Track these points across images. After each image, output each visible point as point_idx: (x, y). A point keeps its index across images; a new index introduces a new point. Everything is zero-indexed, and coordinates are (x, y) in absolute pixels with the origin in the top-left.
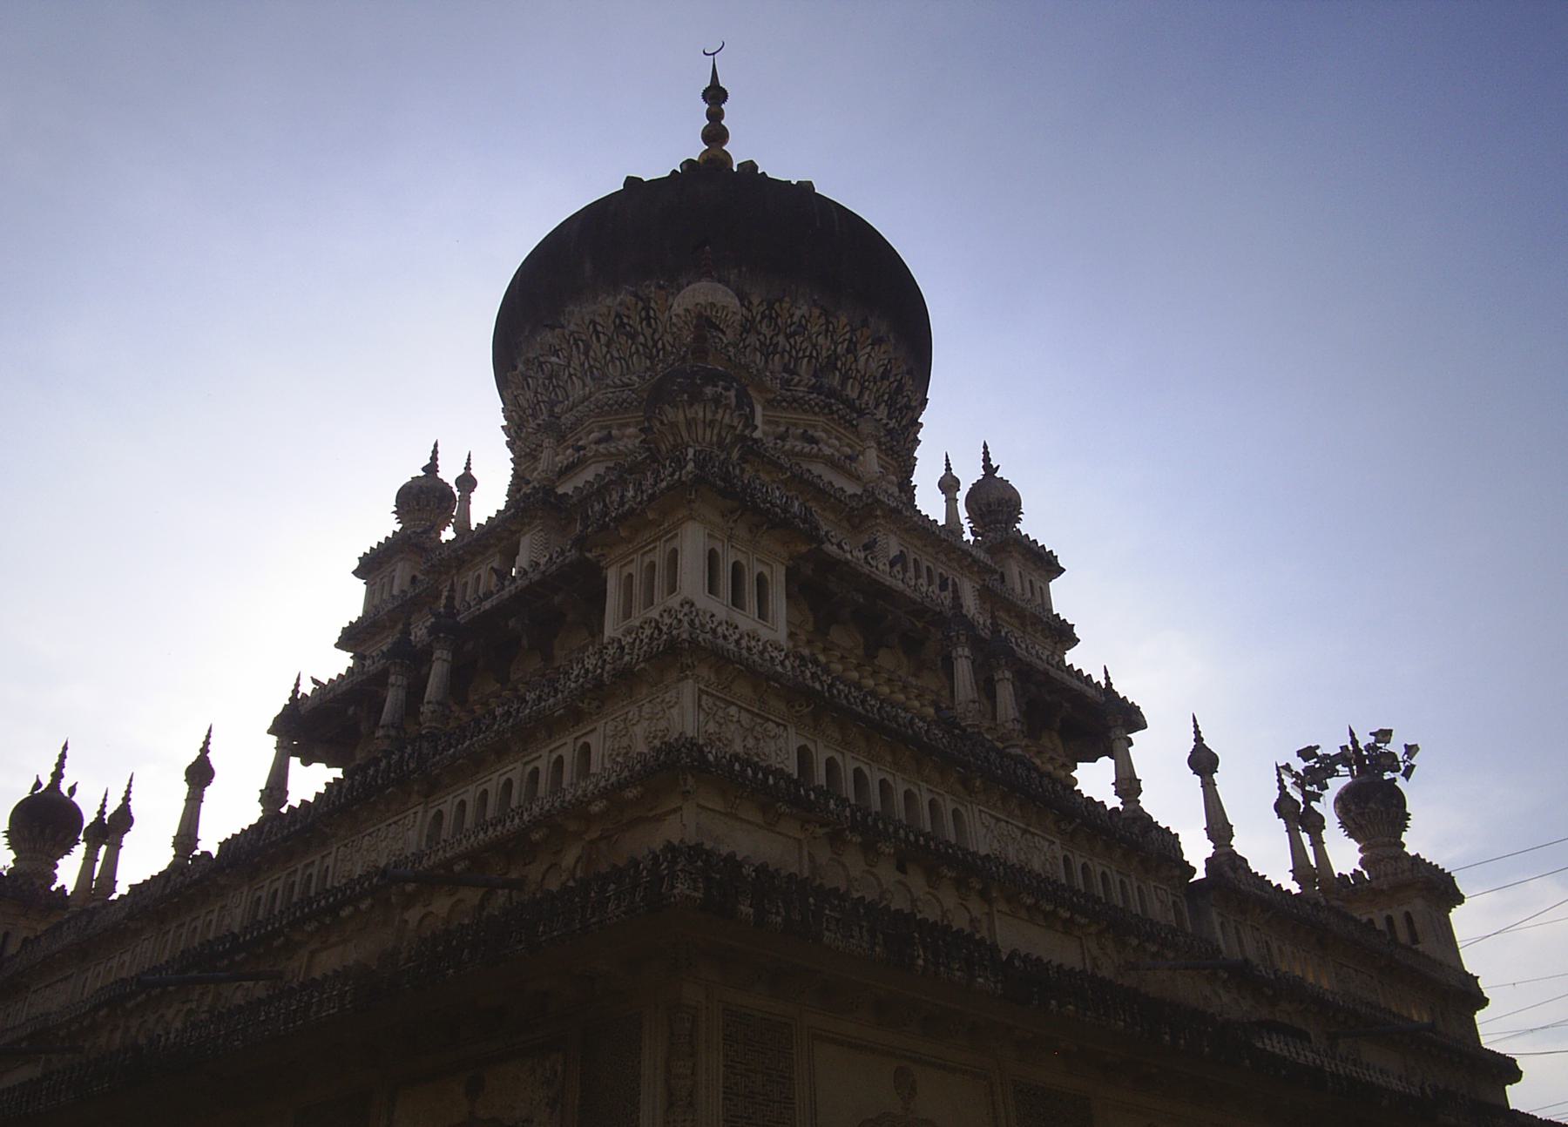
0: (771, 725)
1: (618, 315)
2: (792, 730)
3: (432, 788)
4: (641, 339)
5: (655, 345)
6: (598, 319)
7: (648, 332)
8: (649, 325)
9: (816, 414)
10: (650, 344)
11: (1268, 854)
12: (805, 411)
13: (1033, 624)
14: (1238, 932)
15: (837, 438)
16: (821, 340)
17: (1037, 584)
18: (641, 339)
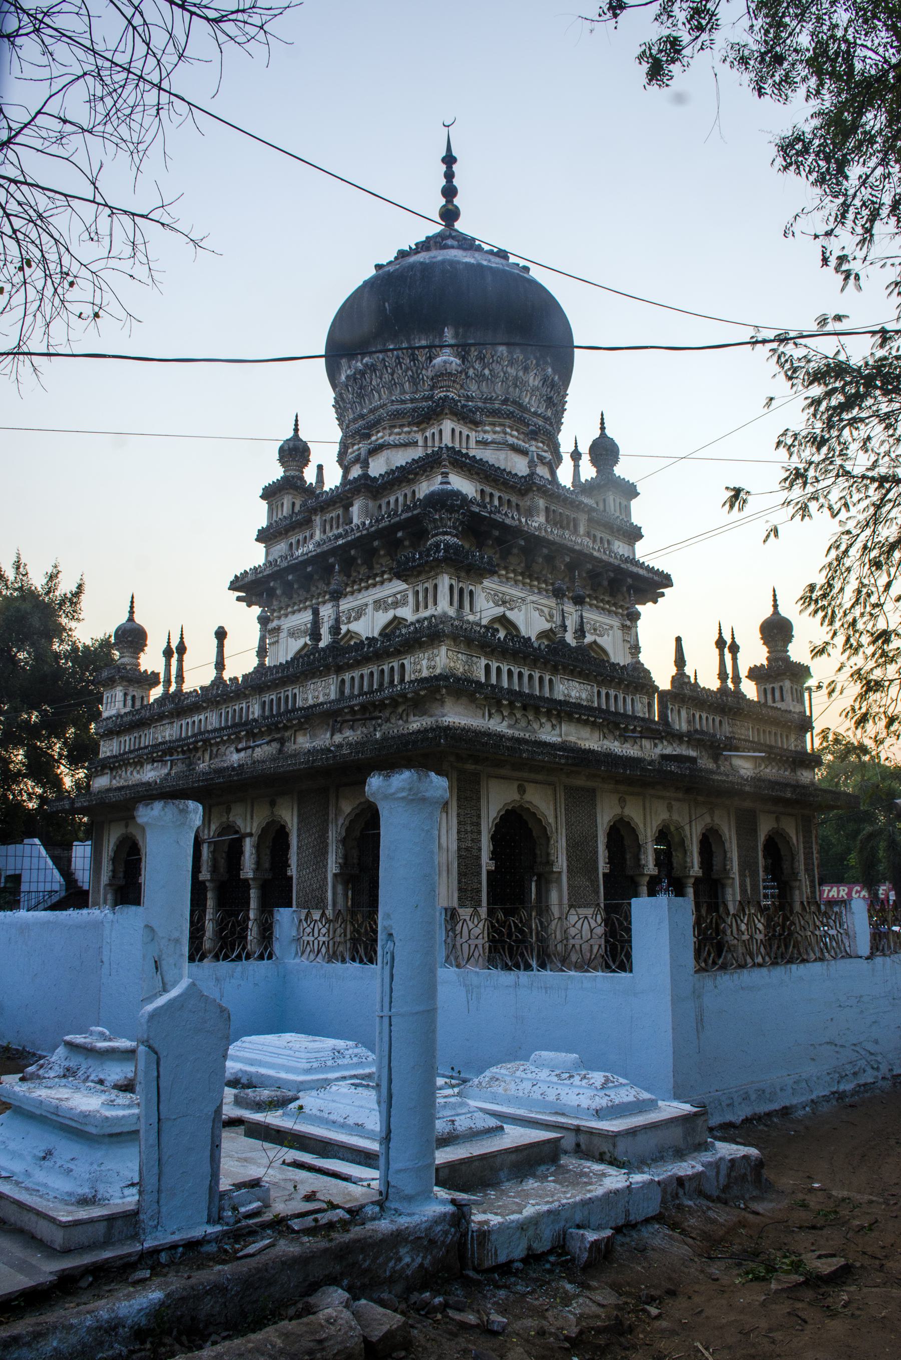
4: (410, 373)
7: (414, 369)
16: (509, 369)
18: (410, 373)
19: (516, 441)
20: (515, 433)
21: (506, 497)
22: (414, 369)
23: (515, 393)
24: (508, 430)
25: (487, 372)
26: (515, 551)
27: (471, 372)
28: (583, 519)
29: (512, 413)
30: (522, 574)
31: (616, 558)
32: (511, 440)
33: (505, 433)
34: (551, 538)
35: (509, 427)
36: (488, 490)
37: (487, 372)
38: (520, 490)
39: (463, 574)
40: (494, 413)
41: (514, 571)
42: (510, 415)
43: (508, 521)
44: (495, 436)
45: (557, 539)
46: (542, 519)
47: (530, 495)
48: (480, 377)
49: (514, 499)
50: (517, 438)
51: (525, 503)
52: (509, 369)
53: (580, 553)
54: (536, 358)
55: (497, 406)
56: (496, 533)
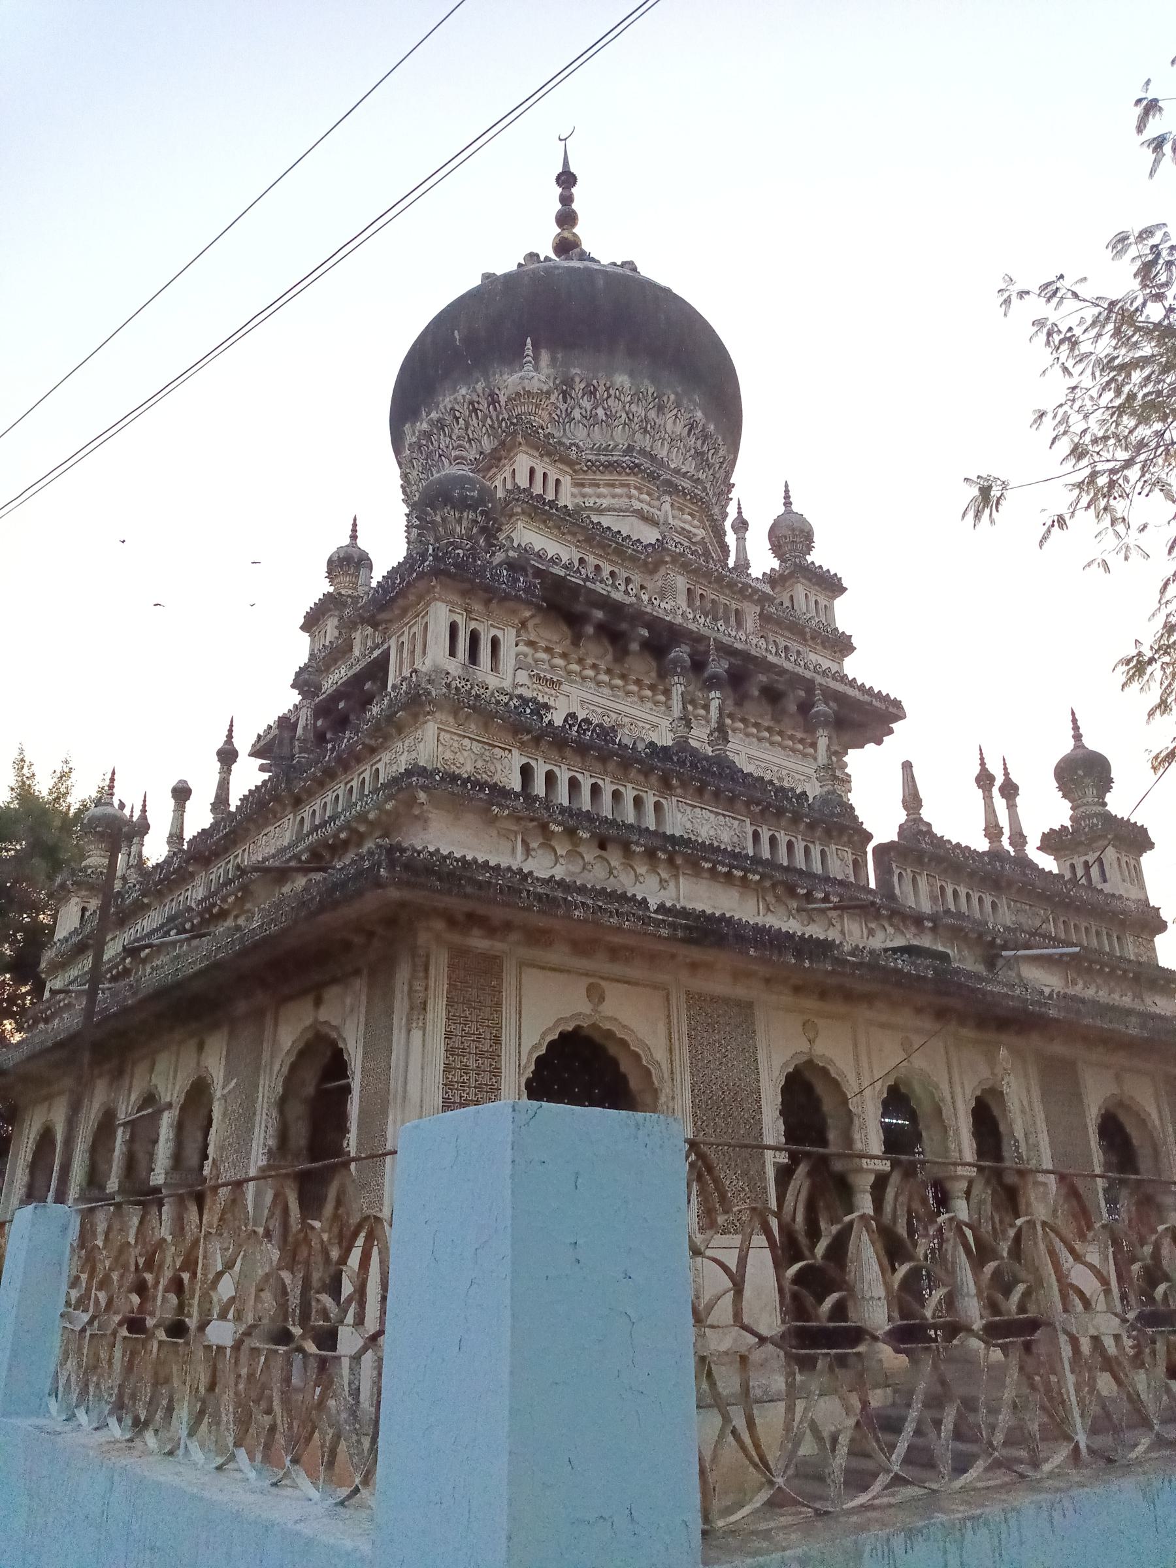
0: (497, 750)
1: (471, 403)
2: (515, 752)
3: (298, 802)
4: (489, 421)
5: (500, 427)
6: (457, 407)
7: (494, 414)
8: (495, 409)
9: (628, 475)
10: (496, 425)
11: (959, 822)
12: (619, 473)
13: (813, 638)
14: (914, 880)
15: (648, 494)
16: (634, 408)
17: (823, 602)
18: (489, 421)
19: (646, 507)
20: (645, 497)
21: (623, 574)
22: (494, 414)
23: (645, 442)
24: (634, 492)
25: (600, 412)
26: (634, 646)
27: (576, 414)
28: (751, 612)
29: (637, 466)
30: (652, 687)
31: (806, 667)
32: (637, 505)
33: (630, 497)
34: (693, 627)
35: (636, 488)
36: (592, 560)
37: (600, 412)
38: (646, 563)
39: (477, 607)
40: (610, 467)
41: (638, 682)
42: (635, 468)
43: (618, 596)
44: (613, 501)
45: (704, 631)
46: (682, 601)
47: (662, 571)
48: (590, 419)
49: (637, 578)
50: (649, 504)
51: (655, 583)
52: (634, 408)
53: (746, 656)
54: (677, 394)
55: (615, 458)
56: (599, 615)
